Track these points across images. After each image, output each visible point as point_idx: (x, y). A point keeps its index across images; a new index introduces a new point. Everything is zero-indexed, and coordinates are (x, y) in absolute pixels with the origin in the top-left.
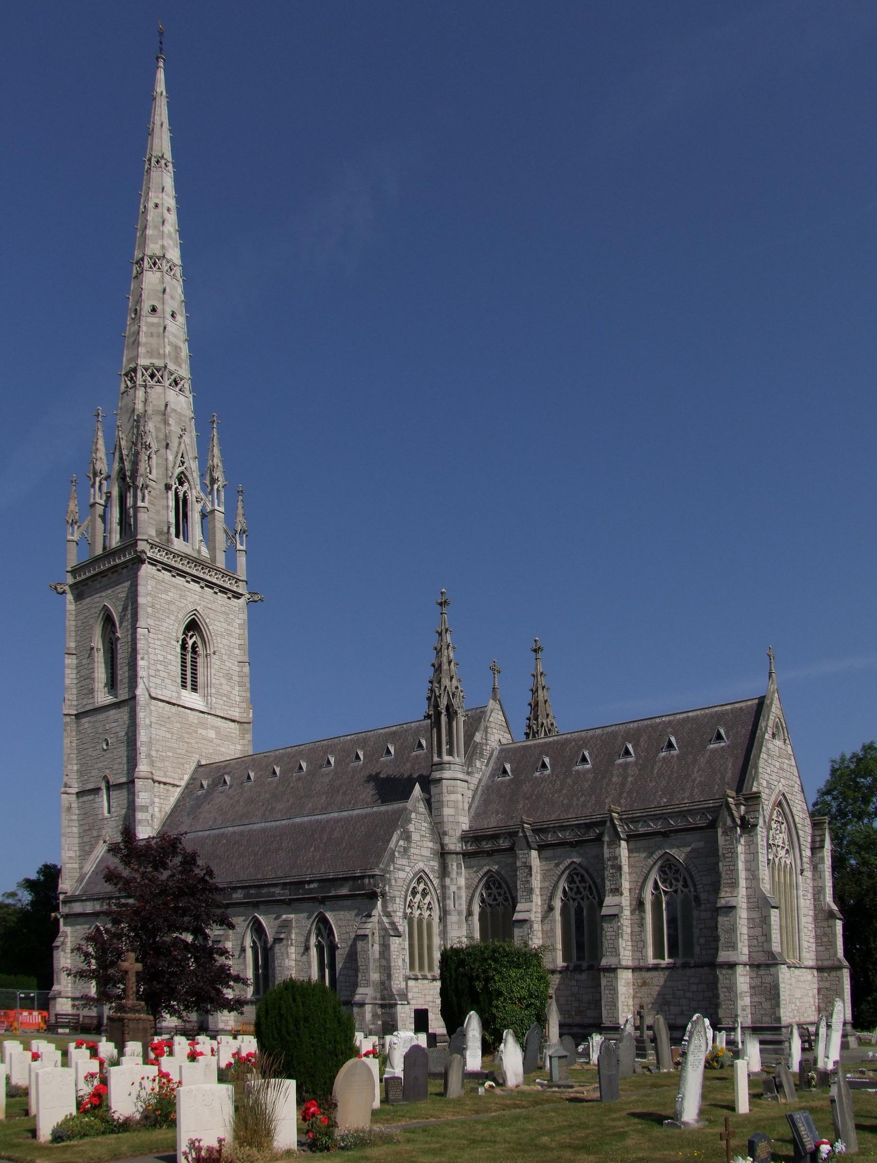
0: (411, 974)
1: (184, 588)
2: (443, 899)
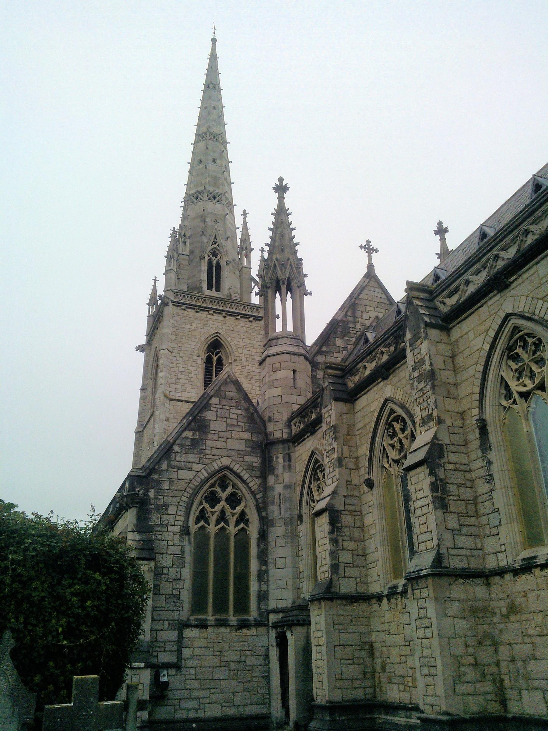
0: (192, 618)
1: (205, 319)
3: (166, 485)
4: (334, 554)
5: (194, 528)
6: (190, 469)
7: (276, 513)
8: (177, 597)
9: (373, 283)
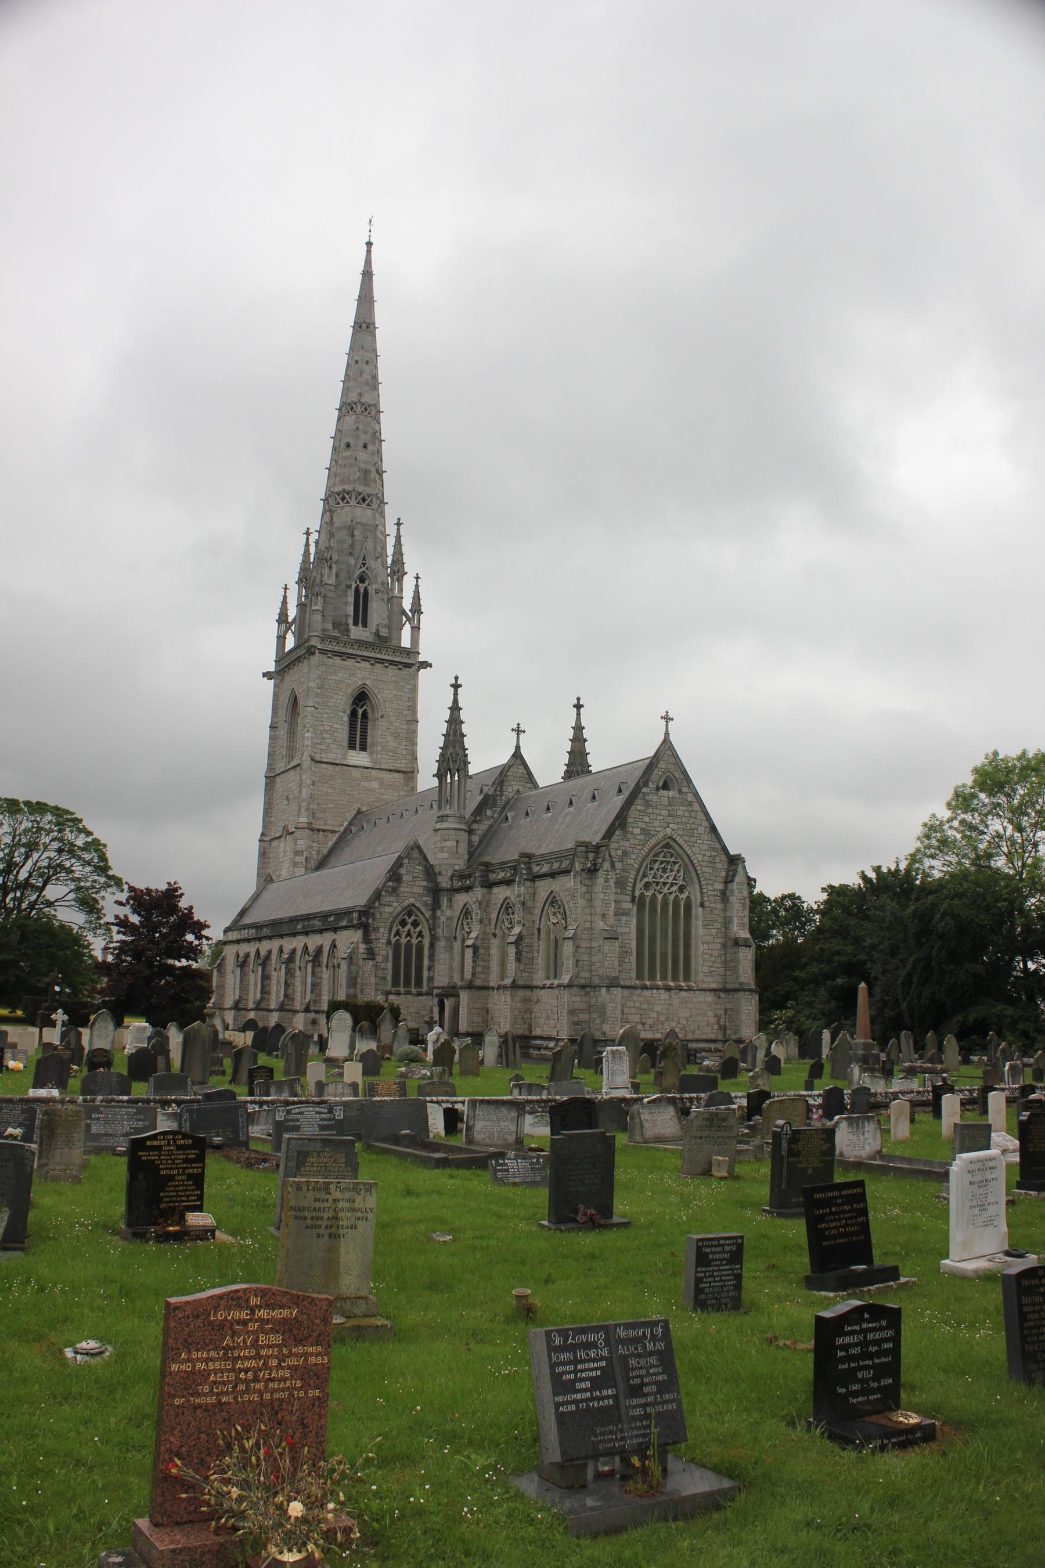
2: (432, 929)
3: (378, 916)
4: (474, 968)
5: (393, 940)
6: (391, 906)
7: (441, 933)
8: (385, 978)
9: (519, 762)
